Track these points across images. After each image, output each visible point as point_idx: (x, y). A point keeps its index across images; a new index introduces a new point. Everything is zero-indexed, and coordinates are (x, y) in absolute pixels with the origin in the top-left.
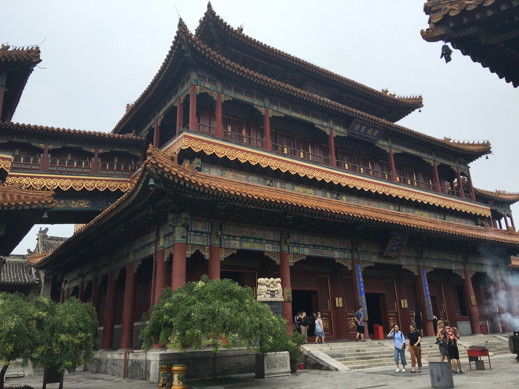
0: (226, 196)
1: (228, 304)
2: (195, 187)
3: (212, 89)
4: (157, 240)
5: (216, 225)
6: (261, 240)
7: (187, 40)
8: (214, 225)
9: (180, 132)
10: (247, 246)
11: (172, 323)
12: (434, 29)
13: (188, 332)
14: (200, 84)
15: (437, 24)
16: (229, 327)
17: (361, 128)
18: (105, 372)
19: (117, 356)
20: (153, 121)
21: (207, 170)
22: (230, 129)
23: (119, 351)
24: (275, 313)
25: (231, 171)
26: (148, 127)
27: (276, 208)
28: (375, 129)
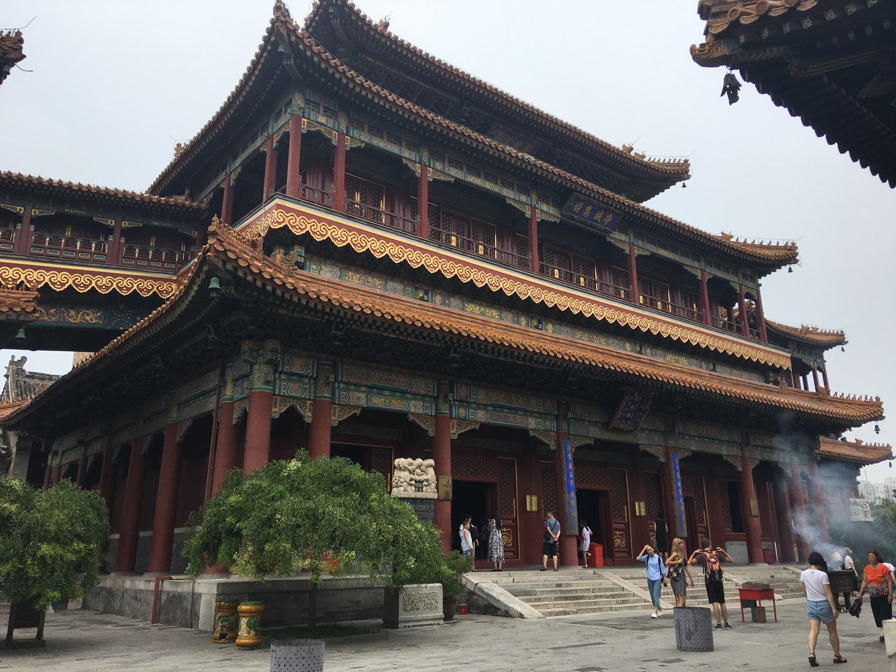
0: (346, 314)
1: (340, 500)
2: (291, 297)
3: (331, 125)
4: (221, 387)
5: (327, 365)
6: (403, 392)
7: (289, 37)
8: (324, 364)
9: (270, 199)
10: (378, 402)
11: (240, 530)
12: (713, 45)
13: (267, 547)
14: (309, 115)
15: (718, 37)
16: (339, 540)
17: (583, 209)
18: (120, 613)
19: (143, 584)
20: (222, 176)
21: (314, 267)
22: (358, 198)
23: (146, 576)
24: (422, 519)
25: (356, 271)
26: (213, 186)
27: (431, 339)
28: (607, 211)
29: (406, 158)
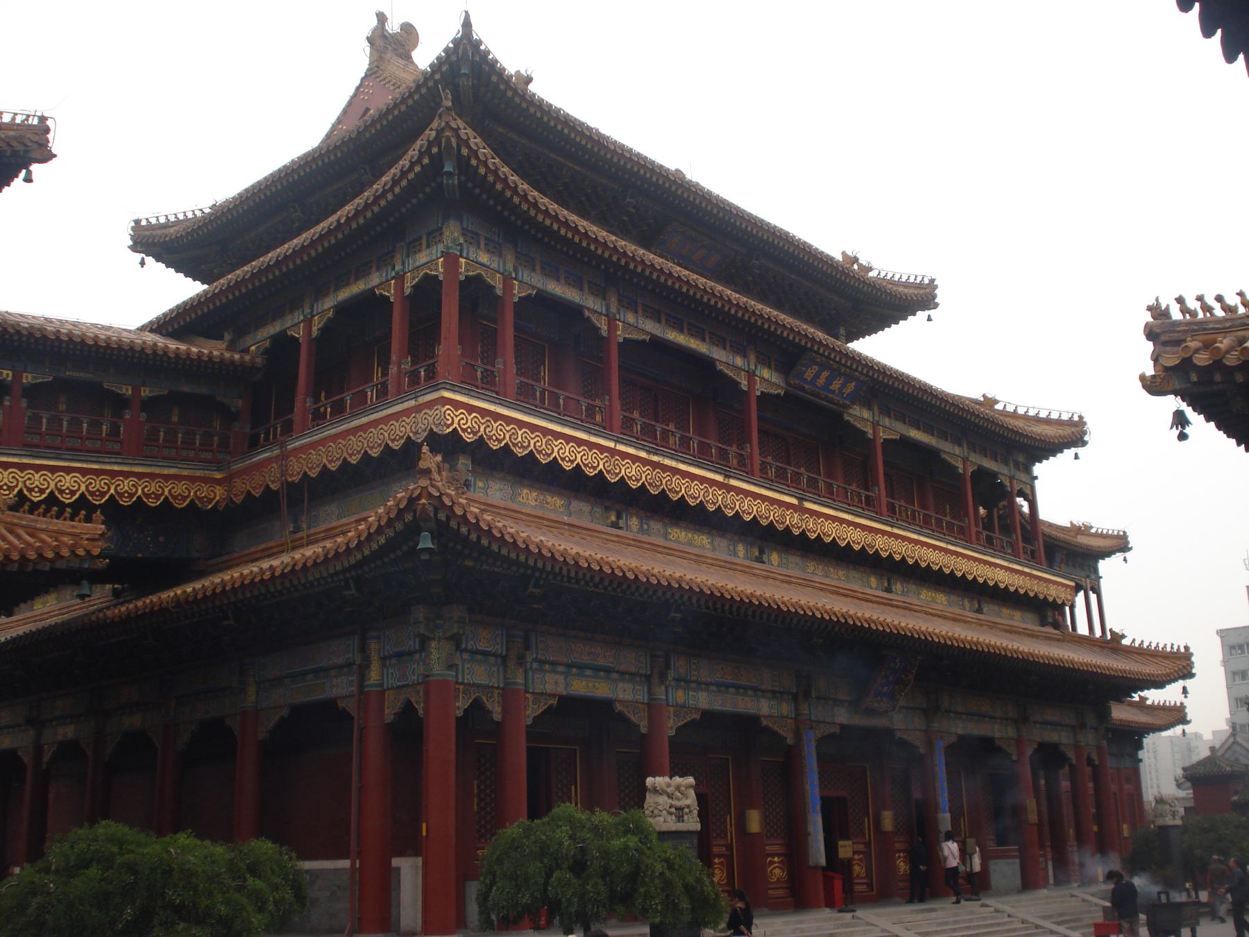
3: (494, 266)
6: (608, 671)
10: (581, 687)
17: (817, 376)
29: (588, 309)
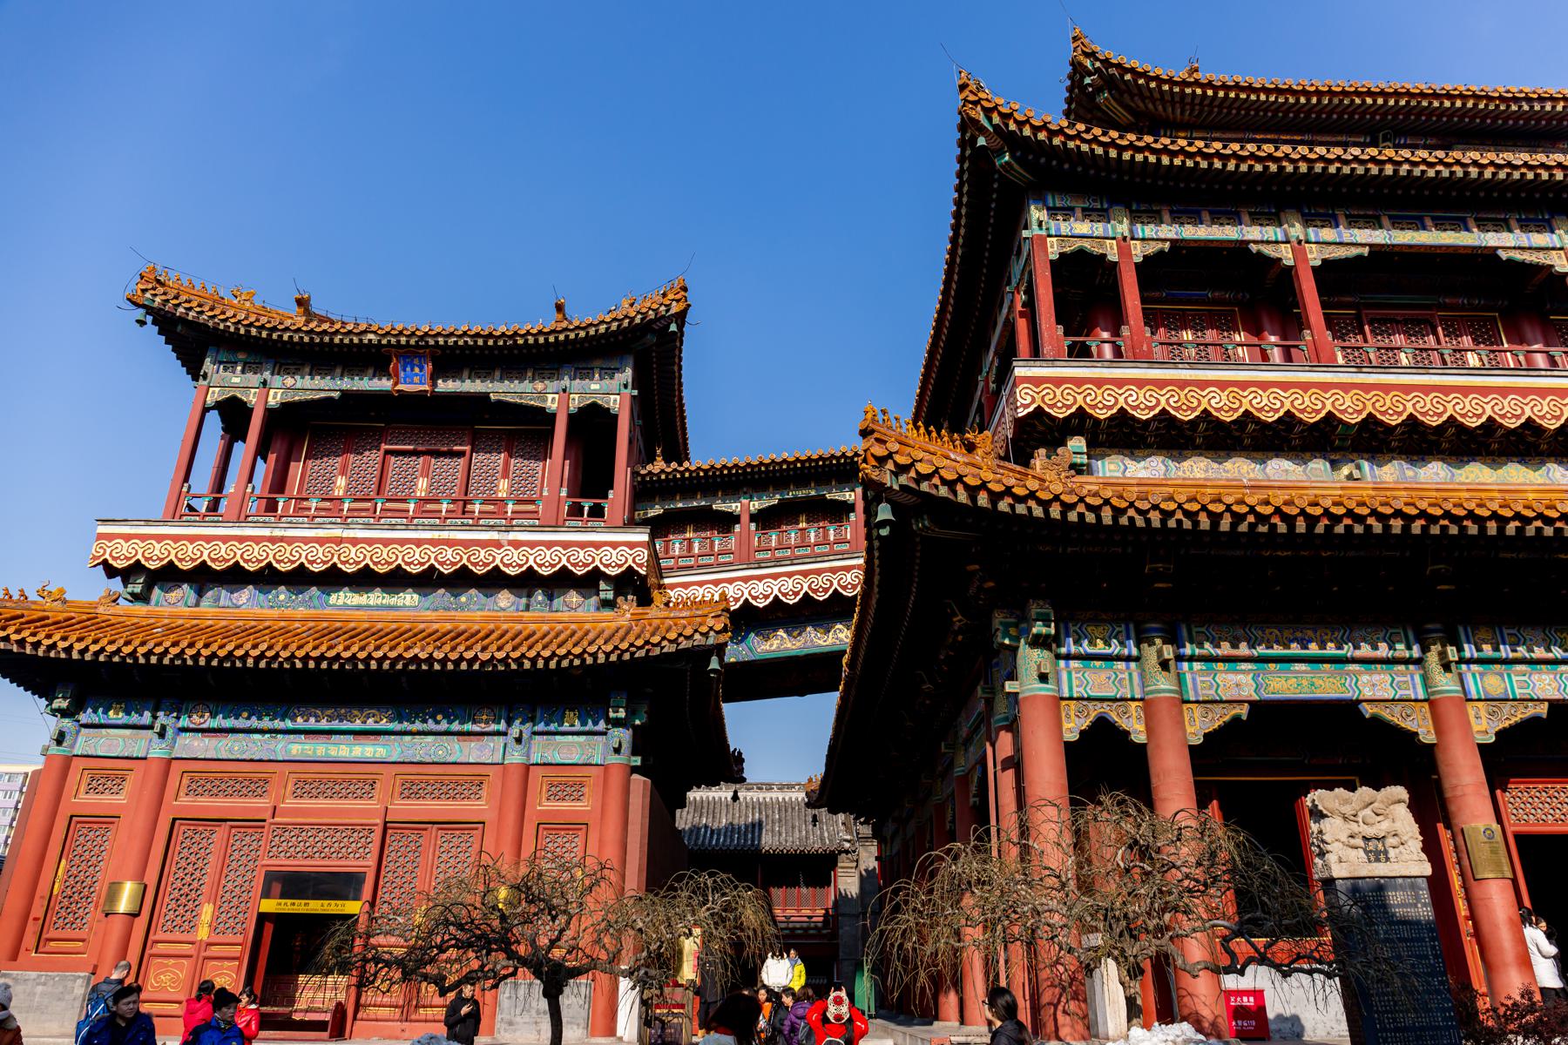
29: (1255, 242)
